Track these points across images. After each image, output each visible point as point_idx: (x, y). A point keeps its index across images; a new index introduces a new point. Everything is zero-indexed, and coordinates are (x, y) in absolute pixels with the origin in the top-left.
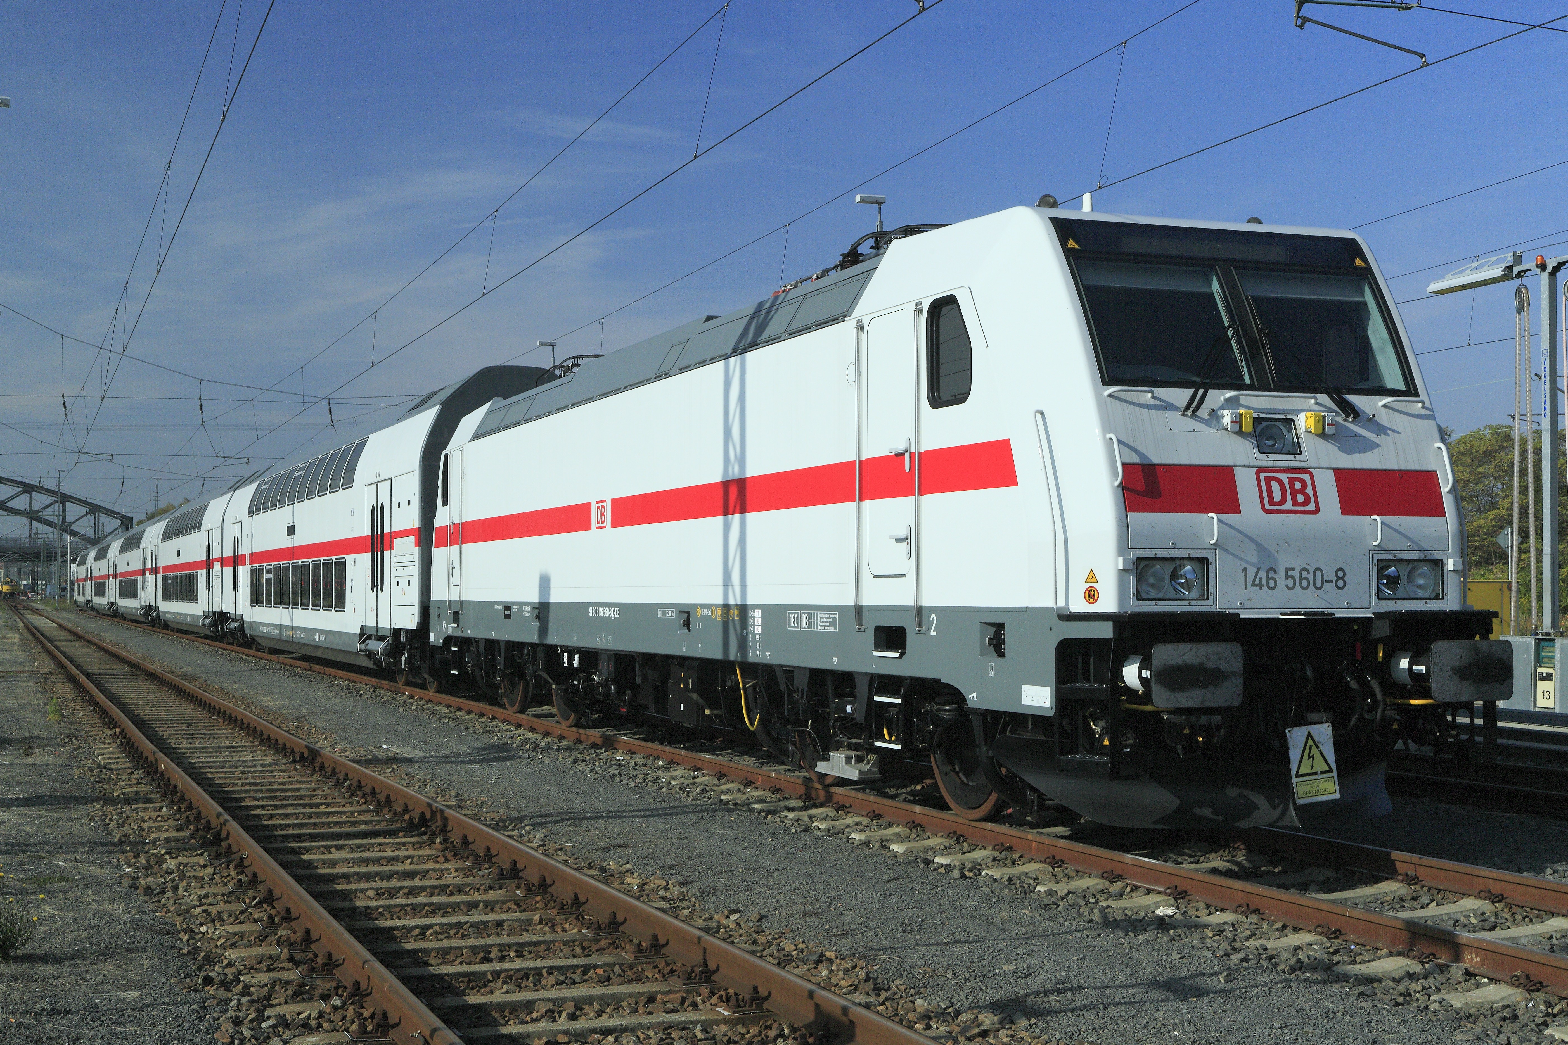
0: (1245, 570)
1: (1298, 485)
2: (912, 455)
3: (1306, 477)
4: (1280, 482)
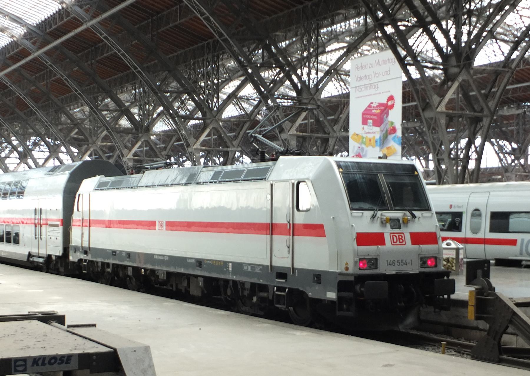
0: (387, 261)
1: (400, 237)
2: (290, 225)
3: (402, 235)
4: (396, 237)
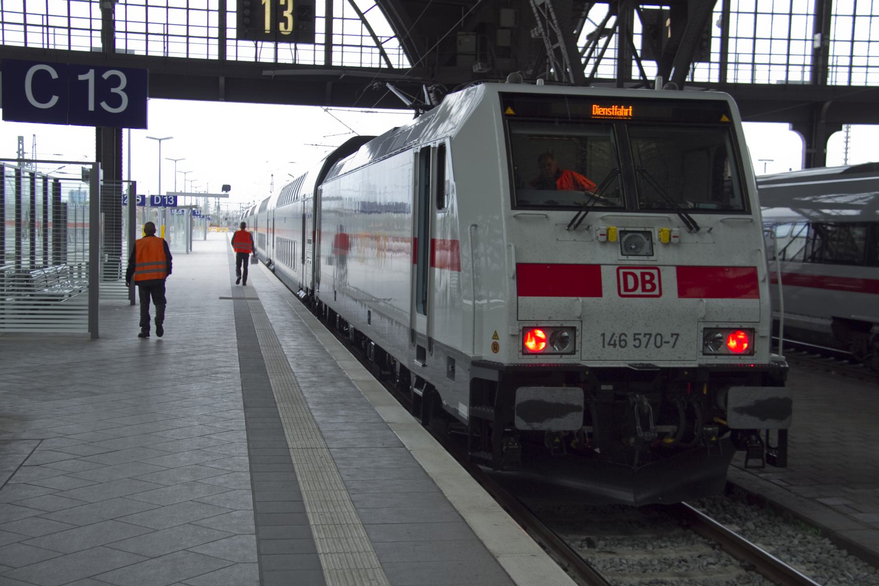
0: (603, 335)
1: (648, 278)
3: (655, 272)
